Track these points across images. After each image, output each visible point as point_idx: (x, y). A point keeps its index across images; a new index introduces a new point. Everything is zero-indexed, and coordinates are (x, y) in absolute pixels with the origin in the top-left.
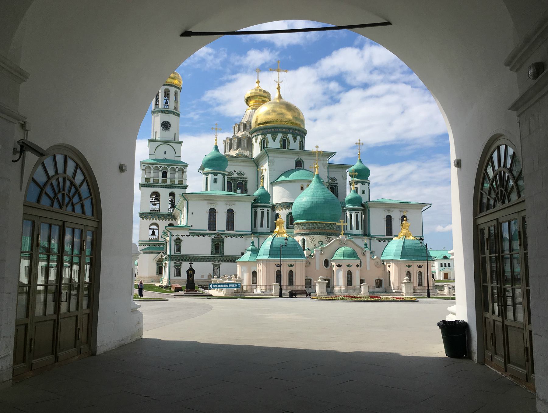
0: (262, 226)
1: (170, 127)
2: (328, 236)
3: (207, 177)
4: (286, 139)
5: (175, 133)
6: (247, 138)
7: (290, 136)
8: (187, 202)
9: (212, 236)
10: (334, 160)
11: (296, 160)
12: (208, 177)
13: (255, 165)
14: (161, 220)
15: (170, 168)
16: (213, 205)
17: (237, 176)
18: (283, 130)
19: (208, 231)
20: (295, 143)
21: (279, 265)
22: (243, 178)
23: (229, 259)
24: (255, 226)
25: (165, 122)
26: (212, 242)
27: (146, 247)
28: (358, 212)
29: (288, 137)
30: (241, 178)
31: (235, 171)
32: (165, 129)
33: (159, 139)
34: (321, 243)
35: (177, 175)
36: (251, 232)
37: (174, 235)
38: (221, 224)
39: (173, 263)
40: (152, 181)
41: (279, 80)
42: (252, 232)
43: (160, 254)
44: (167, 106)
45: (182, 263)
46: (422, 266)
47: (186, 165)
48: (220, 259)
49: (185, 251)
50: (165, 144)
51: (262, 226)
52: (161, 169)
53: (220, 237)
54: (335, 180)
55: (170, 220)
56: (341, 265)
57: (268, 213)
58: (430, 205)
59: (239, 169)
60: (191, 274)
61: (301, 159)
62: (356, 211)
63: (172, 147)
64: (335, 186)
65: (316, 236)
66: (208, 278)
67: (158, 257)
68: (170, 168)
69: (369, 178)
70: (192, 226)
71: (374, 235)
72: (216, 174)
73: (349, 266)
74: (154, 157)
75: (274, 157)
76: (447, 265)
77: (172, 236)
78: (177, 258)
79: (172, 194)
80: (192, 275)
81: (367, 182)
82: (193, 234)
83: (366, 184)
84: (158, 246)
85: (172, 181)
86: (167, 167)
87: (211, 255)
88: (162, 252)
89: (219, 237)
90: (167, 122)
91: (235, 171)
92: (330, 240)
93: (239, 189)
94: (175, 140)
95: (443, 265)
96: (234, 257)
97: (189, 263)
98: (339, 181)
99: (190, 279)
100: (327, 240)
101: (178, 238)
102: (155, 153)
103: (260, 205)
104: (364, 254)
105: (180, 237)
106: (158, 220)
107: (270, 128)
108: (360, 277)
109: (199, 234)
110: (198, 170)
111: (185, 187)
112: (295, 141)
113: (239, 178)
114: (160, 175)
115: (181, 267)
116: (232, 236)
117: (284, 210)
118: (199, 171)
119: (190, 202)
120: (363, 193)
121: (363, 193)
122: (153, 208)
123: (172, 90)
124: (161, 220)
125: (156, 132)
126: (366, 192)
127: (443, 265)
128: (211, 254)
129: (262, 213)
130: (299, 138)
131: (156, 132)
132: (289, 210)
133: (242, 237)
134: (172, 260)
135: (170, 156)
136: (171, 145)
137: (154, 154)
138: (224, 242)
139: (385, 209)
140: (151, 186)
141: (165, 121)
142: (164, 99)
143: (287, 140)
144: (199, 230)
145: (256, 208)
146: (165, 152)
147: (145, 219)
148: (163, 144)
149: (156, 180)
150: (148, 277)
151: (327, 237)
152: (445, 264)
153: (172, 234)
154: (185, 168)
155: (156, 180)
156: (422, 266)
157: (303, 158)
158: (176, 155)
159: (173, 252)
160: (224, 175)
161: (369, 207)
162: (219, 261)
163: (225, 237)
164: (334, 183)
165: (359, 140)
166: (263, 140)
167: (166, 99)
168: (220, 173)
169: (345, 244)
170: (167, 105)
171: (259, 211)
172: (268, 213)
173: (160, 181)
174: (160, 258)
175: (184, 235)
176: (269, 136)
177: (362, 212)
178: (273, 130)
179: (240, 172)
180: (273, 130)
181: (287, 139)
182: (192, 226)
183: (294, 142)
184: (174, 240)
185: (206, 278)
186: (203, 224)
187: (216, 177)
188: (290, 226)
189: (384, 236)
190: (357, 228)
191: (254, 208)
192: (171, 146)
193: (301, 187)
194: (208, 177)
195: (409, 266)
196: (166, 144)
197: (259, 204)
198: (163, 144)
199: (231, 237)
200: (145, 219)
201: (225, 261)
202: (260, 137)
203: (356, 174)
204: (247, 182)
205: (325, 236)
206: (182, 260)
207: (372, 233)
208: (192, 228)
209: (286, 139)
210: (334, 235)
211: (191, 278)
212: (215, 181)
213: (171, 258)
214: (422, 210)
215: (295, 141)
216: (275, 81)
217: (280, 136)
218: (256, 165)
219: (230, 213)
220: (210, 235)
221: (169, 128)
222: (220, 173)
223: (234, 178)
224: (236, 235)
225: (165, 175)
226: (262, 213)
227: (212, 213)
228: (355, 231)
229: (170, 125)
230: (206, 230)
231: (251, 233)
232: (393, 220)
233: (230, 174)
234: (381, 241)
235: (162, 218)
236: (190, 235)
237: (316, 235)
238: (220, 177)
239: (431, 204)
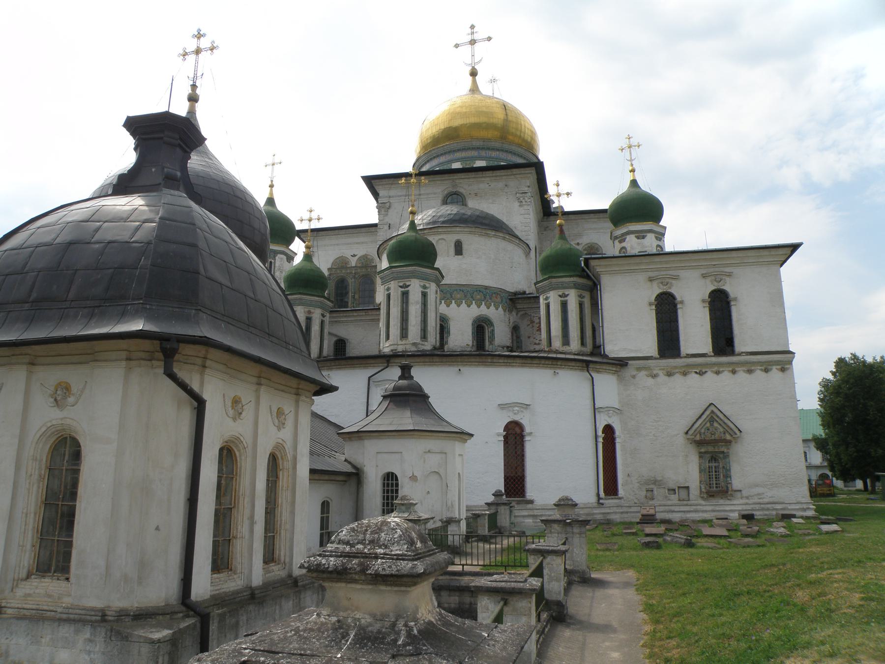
59: (360, 252)
69: (660, 224)
75: (390, 197)
81: (650, 231)
91: (354, 256)
232: (679, 306)
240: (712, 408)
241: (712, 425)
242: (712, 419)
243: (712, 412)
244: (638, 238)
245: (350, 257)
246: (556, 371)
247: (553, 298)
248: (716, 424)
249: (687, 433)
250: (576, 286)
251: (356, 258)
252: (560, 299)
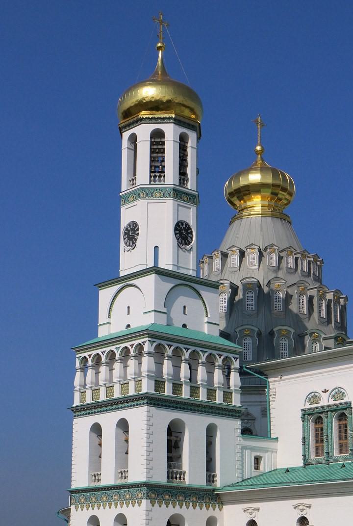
25: (182, 225)
32: (182, 243)
33: (170, 268)
35: (218, 376)
50: (187, 285)
79: (211, 433)
106: (184, 507)
125: (156, 248)
131: (156, 248)
137: (165, 310)
140: (175, 405)
141: (182, 222)
147: (156, 505)
148: (181, 285)
154: (236, 359)
173: (185, 393)
196: (187, 285)
198: (181, 285)
200: (156, 505)
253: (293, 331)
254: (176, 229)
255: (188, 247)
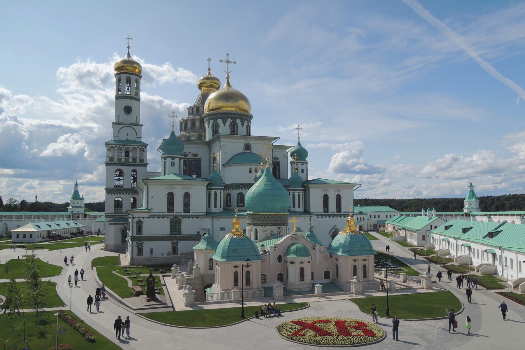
0: (215, 207)
1: (132, 111)
2: (279, 226)
3: (165, 160)
4: (235, 124)
5: (136, 117)
6: (200, 120)
7: (238, 121)
8: (148, 186)
9: (171, 217)
10: (277, 143)
11: (245, 144)
12: (166, 161)
13: (207, 147)
14: (125, 195)
15: (132, 148)
16: (171, 189)
17: (192, 157)
18: (233, 116)
19: (167, 213)
20: (243, 127)
21: (236, 267)
22: (198, 159)
23: (187, 238)
24: (209, 207)
26: (171, 223)
27: (112, 218)
28: (300, 192)
29: (237, 121)
30: (195, 159)
31: (190, 152)
32: (127, 113)
34: (272, 233)
35: (138, 155)
36: (205, 212)
37: (135, 218)
38: (179, 207)
39: (135, 243)
40: (116, 160)
41: (228, 70)
42: (206, 213)
43: (125, 225)
44: (129, 92)
45: (143, 243)
46: (366, 260)
47: (146, 145)
48: (178, 238)
49: (146, 231)
50: (127, 126)
51: (215, 207)
52: (123, 149)
53: (178, 218)
54: (277, 159)
55: (133, 195)
56: (294, 262)
57: (221, 194)
58: (360, 185)
60: (151, 281)
61: (249, 143)
62: (298, 192)
63: (134, 129)
64: (277, 164)
65: (267, 227)
66: (168, 255)
67: (124, 227)
68: (132, 148)
70: (152, 208)
71: (313, 212)
72: (173, 158)
73: (302, 263)
74: (117, 139)
76: (362, 219)
77: (134, 218)
78: (139, 238)
80: (152, 282)
81: (305, 163)
82: (153, 216)
83: (305, 164)
84: (122, 218)
85: (134, 160)
86: (130, 148)
87: (170, 235)
88: (126, 223)
89: (176, 218)
90: (129, 106)
91: (190, 152)
92: (281, 229)
93: (194, 174)
94: (136, 123)
95: (359, 219)
96: (190, 236)
97: (149, 271)
98: (281, 160)
99: (151, 286)
100: (278, 230)
101: (139, 220)
102: (118, 134)
103: (214, 188)
104: (314, 248)
105: (141, 219)
106: (122, 194)
107: (221, 114)
108: (311, 270)
109: (158, 216)
110: (157, 149)
111: (145, 165)
112: (243, 124)
113: (193, 159)
114: (123, 154)
115: (142, 247)
116: (188, 217)
117: (234, 190)
118: (158, 150)
119: (150, 187)
120: (302, 172)
121: (302, 172)
122: (117, 184)
123: (133, 78)
124: (125, 195)
125: (119, 115)
126: (305, 171)
127: (359, 219)
128: (169, 234)
129: (216, 195)
130: (246, 122)
131: (119, 115)
132: (239, 190)
133: (197, 218)
134: (135, 240)
135: (131, 137)
136: (134, 128)
137: (118, 135)
138: (181, 223)
139: (322, 189)
141: (127, 106)
142: (126, 86)
143: (236, 124)
144: (158, 212)
145: (210, 191)
146: (127, 133)
147: (110, 194)
148: (126, 126)
149: (119, 159)
150: (113, 245)
151: (278, 227)
152: (361, 218)
153: (134, 217)
155: (119, 159)
156: (366, 260)
157: (251, 142)
158: (137, 136)
159: (135, 233)
160: (180, 159)
161: (309, 188)
162: (177, 240)
163: (182, 218)
164: (277, 162)
165: (301, 129)
166: (215, 124)
167: (128, 86)
168: (177, 157)
169: (296, 240)
170: (129, 91)
171: (213, 193)
172: (221, 194)
173: (123, 160)
174: (124, 229)
175: (145, 218)
176: (220, 121)
177: (303, 192)
178: (223, 116)
179: (194, 154)
180: (223, 116)
181: (236, 123)
182: (152, 208)
183: (242, 126)
184: (136, 222)
185: (165, 255)
186: (162, 206)
187: (173, 161)
188: (240, 204)
189: (322, 213)
190: (299, 207)
191: (209, 191)
192: (133, 128)
193: (250, 170)
194: (166, 161)
195: (355, 261)
196: (128, 126)
197: (212, 187)
198: (126, 126)
199: (188, 218)
200: (110, 194)
201: (182, 240)
202: (212, 121)
203: (298, 158)
204: (201, 162)
205: (276, 226)
206: (143, 240)
207: (312, 211)
208: (152, 211)
209: (235, 124)
210: (284, 225)
211: (151, 285)
212: (173, 164)
213: (133, 238)
214: (354, 189)
215: (243, 124)
216: (225, 71)
217: (229, 121)
218: (209, 147)
219: (187, 196)
220: (169, 217)
221: (131, 112)
222: (177, 157)
223: (189, 158)
224: (193, 216)
225: (127, 154)
226: (216, 195)
227: (171, 197)
228: (297, 209)
229: (132, 109)
230: (165, 212)
231: (206, 214)
232: (329, 198)
233: (185, 155)
234: (319, 217)
235: (125, 193)
236: (150, 218)
237: (268, 225)
238: (177, 161)
239: (361, 184)
240: (336, 227)
241: (335, 231)
242: (335, 229)
243: (336, 228)
244: (302, 164)
245: (188, 153)
246: (305, 218)
247: (296, 193)
248: (336, 231)
249: (330, 232)
250: (303, 190)
251: (191, 153)
252: (298, 193)
253: (197, 134)
254: (124, 108)
255: (130, 114)
